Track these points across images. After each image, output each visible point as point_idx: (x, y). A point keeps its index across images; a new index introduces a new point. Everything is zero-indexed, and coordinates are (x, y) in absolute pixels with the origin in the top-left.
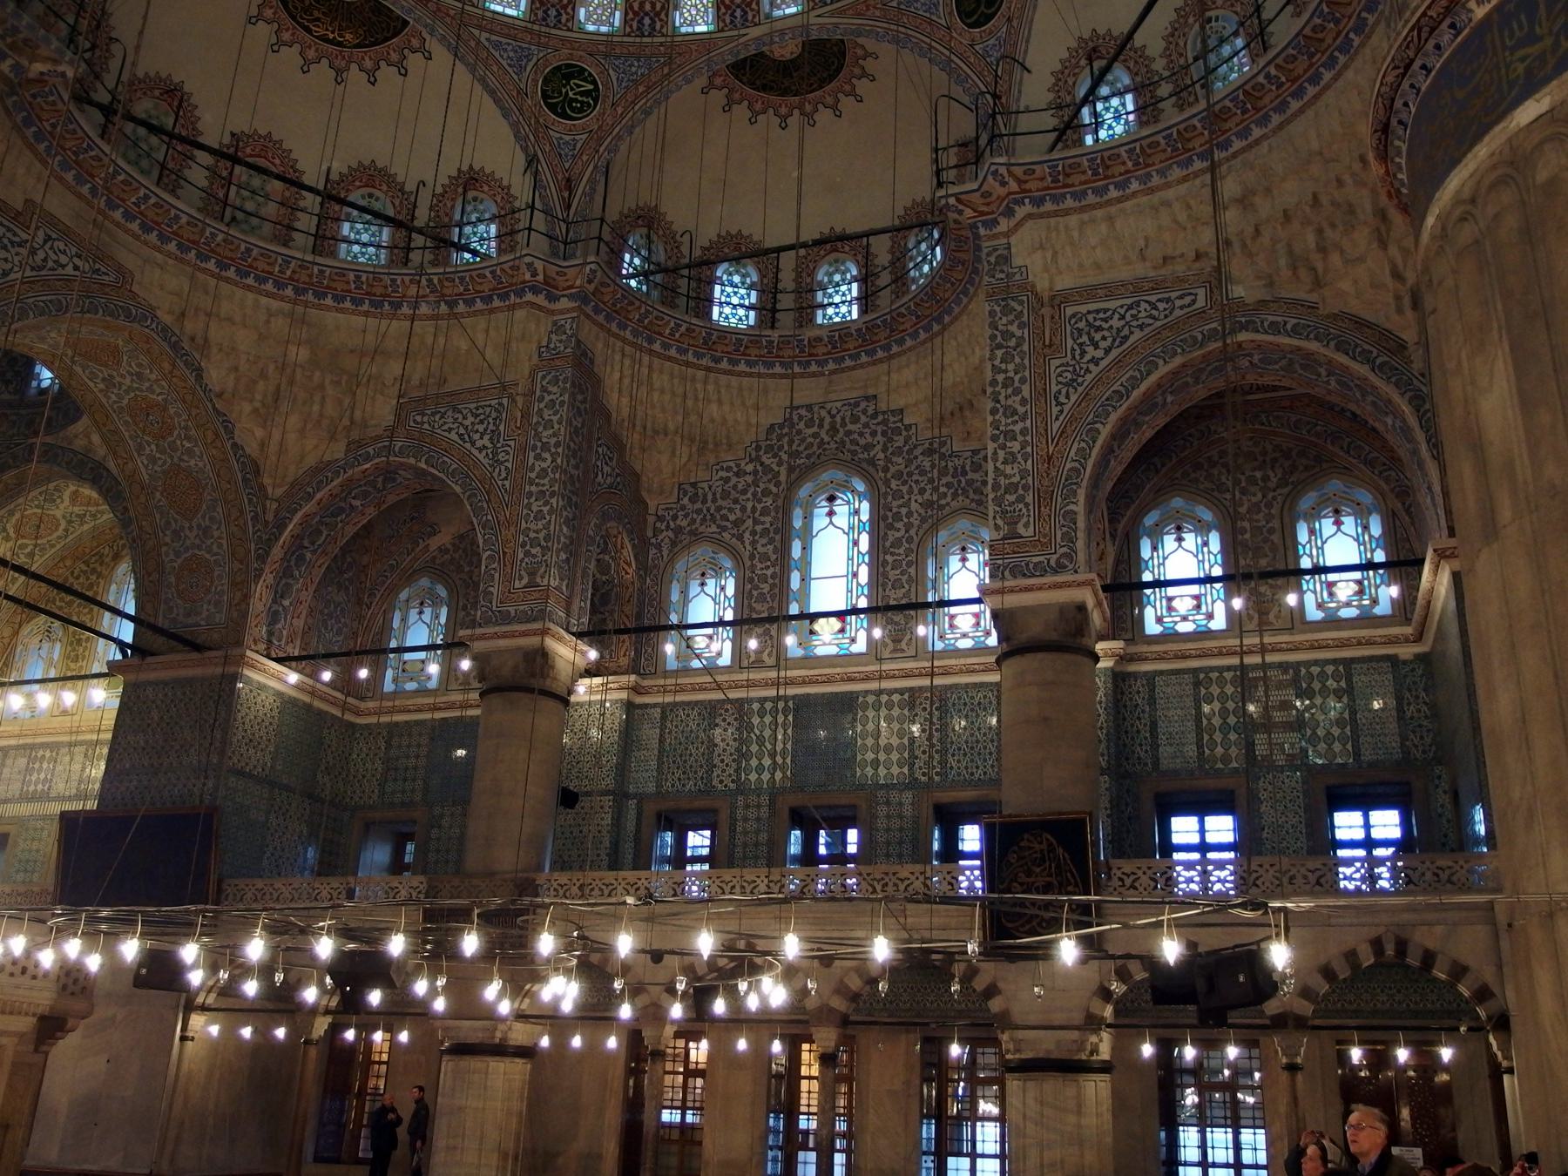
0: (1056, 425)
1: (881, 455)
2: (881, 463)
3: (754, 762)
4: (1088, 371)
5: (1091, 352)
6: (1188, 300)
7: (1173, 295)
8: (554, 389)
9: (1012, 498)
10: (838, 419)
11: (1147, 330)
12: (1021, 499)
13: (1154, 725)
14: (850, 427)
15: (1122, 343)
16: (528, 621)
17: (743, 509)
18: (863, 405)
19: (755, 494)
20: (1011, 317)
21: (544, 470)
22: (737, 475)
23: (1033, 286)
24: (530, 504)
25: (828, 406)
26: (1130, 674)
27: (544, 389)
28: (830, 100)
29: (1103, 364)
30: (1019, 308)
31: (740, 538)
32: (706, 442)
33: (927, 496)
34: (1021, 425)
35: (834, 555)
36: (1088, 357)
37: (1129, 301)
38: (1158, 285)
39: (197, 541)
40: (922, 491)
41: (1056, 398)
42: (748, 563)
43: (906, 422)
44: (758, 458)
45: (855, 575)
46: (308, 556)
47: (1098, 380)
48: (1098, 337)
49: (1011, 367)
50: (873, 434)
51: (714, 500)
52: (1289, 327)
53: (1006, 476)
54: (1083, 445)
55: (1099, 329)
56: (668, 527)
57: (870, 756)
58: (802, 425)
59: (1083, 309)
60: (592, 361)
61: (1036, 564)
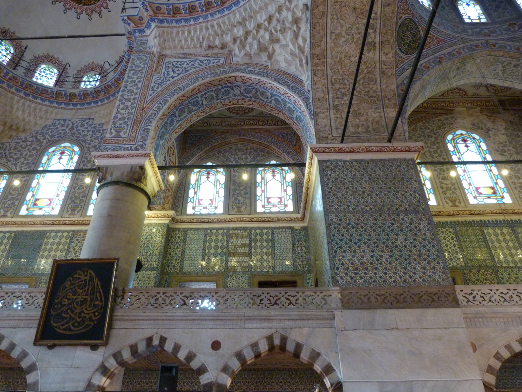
0: (149, 98)
1: (89, 139)
2: (89, 142)
4: (169, 80)
6: (216, 61)
10: (75, 125)
11: (197, 69)
13: (183, 252)
14: (79, 128)
17: (21, 154)
18: (87, 121)
19: (28, 149)
22: (24, 141)
26: (176, 229)
28: (98, 10)
29: (176, 78)
32: (12, 126)
34: (134, 96)
36: (170, 76)
38: (205, 56)
43: (104, 128)
47: (173, 83)
49: (136, 77)
51: (10, 150)
52: (256, 72)
53: (121, 114)
54: (160, 105)
55: (176, 67)
58: (59, 126)
59: (172, 61)
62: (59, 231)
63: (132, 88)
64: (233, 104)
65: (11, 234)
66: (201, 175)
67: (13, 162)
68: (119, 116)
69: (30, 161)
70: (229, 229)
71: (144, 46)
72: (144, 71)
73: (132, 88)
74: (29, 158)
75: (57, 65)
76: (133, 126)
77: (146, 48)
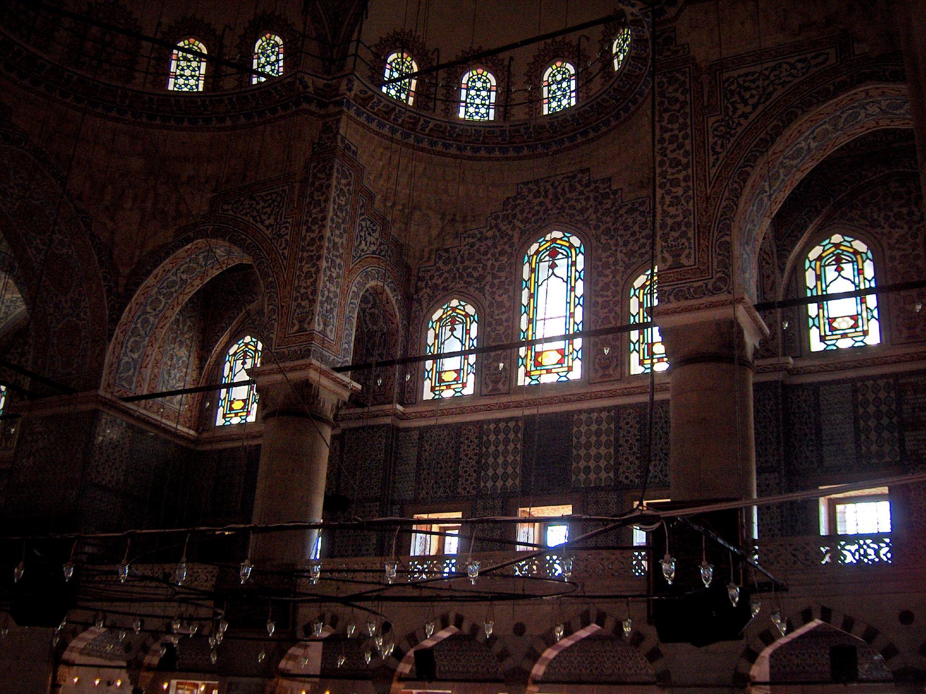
0: (713, 171)
1: (594, 217)
3: (491, 472)
4: (739, 124)
5: (741, 108)
7: (809, 56)
8: (323, 176)
9: (676, 234)
12: (684, 234)
15: (767, 99)
16: (298, 359)
18: (579, 176)
19: (493, 255)
20: (677, 86)
21: (313, 239)
22: (480, 240)
23: (694, 59)
24: (301, 267)
25: (551, 180)
27: (315, 176)
29: (752, 117)
30: (682, 78)
31: (481, 290)
33: (630, 247)
35: (554, 300)
36: (739, 112)
37: (772, 64)
39: (71, 311)
40: (626, 244)
41: (713, 149)
42: (488, 310)
43: (614, 187)
44: (496, 225)
45: (572, 315)
46: (151, 319)
48: (747, 95)
49: (676, 126)
50: (587, 199)
53: (671, 217)
54: (736, 185)
55: (748, 89)
56: (426, 285)
57: (582, 464)
59: (735, 74)
60: (355, 153)
61: (696, 289)
62: (592, 410)
63: (675, 155)
64: (868, 129)
65: (517, 421)
66: (825, 266)
67: (476, 286)
68: (670, 222)
69: (503, 279)
70: (897, 376)
71: (673, 47)
72: (688, 110)
73: (675, 155)
74: (499, 274)
75: (490, 64)
76: (699, 240)
77: (678, 51)
